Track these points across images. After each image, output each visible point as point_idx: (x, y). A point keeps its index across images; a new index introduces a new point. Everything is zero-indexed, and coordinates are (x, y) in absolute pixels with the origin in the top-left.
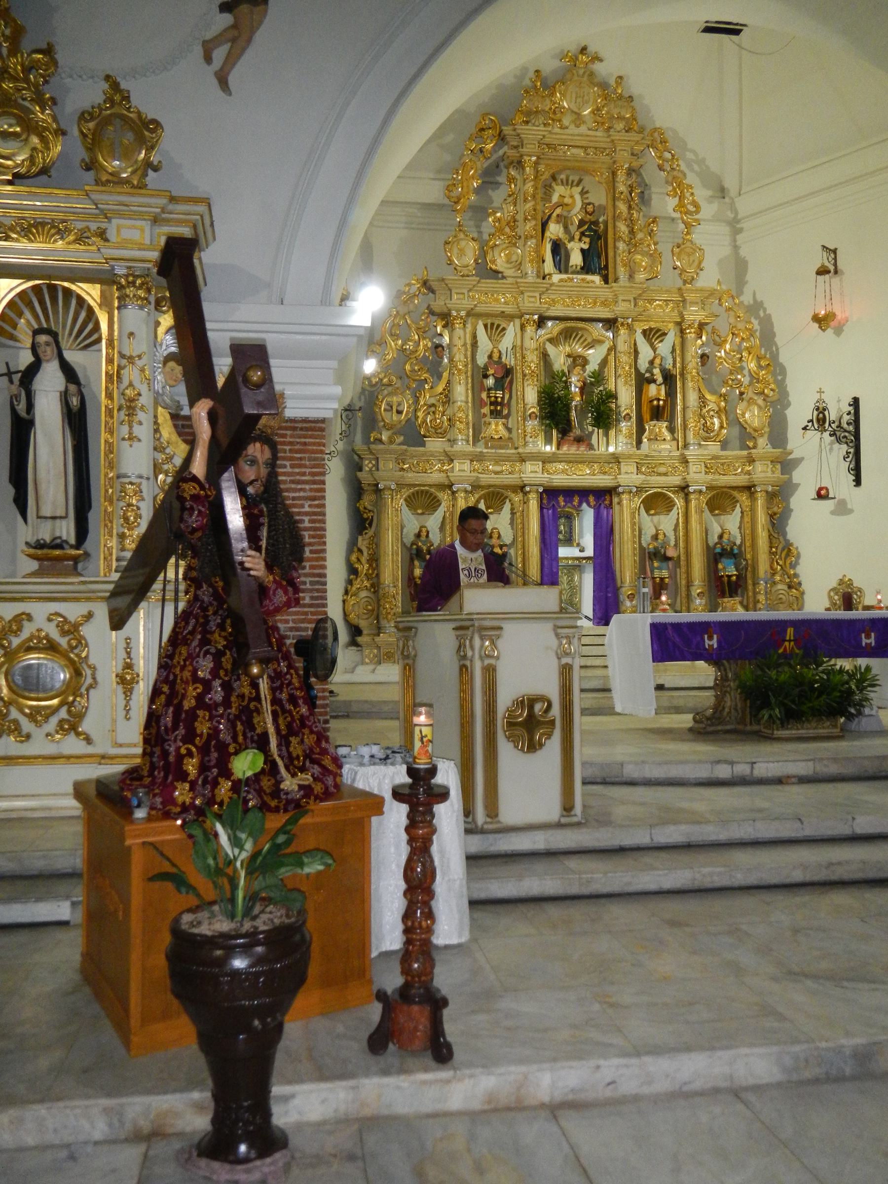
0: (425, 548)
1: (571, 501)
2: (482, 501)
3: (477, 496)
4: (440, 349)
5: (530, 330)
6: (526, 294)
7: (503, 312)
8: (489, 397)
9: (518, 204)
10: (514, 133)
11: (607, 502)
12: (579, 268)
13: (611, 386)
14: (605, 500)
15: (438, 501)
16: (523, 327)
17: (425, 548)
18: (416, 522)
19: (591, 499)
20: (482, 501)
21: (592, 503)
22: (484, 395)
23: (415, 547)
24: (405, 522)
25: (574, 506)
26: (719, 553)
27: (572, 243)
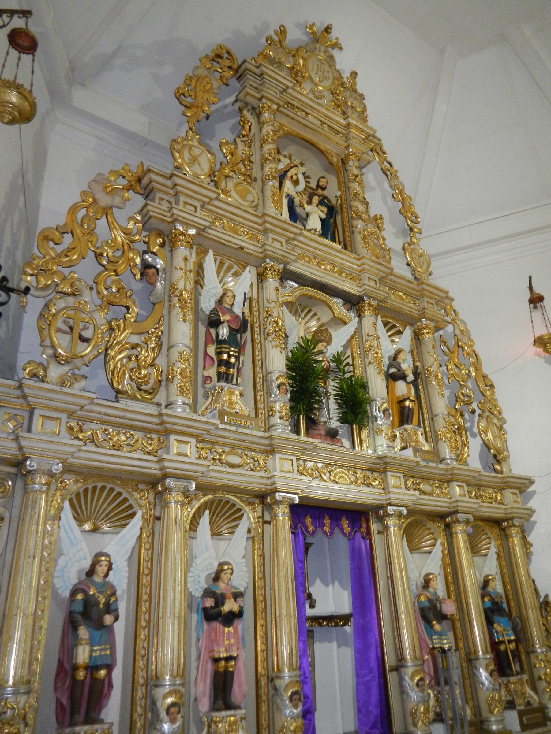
0: (102, 600)
1: (322, 525)
2: (207, 512)
3: (197, 505)
4: (153, 270)
5: (272, 282)
6: (271, 235)
7: (242, 248)
8: (219, 354)
9: (253, 147)
10: (257, 71)
11: (364, 530)
12: (318, 233)
13: (359, 372)
14: (361, 526)
15: (131, 507)
16: (261, 277)
17: (102, 600)
18: (84, 545)
19: (345, 523)
20: (207, 512)
21: (347, 530)
22: (212, 350)
23: (80, 597)
24: (65, 544)
25: (325, 532)
26: (490, 608)
27: (310, 207)
